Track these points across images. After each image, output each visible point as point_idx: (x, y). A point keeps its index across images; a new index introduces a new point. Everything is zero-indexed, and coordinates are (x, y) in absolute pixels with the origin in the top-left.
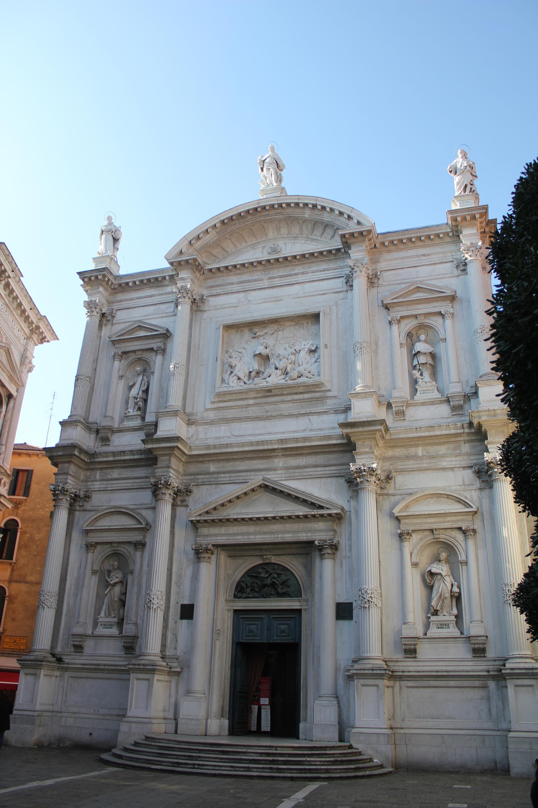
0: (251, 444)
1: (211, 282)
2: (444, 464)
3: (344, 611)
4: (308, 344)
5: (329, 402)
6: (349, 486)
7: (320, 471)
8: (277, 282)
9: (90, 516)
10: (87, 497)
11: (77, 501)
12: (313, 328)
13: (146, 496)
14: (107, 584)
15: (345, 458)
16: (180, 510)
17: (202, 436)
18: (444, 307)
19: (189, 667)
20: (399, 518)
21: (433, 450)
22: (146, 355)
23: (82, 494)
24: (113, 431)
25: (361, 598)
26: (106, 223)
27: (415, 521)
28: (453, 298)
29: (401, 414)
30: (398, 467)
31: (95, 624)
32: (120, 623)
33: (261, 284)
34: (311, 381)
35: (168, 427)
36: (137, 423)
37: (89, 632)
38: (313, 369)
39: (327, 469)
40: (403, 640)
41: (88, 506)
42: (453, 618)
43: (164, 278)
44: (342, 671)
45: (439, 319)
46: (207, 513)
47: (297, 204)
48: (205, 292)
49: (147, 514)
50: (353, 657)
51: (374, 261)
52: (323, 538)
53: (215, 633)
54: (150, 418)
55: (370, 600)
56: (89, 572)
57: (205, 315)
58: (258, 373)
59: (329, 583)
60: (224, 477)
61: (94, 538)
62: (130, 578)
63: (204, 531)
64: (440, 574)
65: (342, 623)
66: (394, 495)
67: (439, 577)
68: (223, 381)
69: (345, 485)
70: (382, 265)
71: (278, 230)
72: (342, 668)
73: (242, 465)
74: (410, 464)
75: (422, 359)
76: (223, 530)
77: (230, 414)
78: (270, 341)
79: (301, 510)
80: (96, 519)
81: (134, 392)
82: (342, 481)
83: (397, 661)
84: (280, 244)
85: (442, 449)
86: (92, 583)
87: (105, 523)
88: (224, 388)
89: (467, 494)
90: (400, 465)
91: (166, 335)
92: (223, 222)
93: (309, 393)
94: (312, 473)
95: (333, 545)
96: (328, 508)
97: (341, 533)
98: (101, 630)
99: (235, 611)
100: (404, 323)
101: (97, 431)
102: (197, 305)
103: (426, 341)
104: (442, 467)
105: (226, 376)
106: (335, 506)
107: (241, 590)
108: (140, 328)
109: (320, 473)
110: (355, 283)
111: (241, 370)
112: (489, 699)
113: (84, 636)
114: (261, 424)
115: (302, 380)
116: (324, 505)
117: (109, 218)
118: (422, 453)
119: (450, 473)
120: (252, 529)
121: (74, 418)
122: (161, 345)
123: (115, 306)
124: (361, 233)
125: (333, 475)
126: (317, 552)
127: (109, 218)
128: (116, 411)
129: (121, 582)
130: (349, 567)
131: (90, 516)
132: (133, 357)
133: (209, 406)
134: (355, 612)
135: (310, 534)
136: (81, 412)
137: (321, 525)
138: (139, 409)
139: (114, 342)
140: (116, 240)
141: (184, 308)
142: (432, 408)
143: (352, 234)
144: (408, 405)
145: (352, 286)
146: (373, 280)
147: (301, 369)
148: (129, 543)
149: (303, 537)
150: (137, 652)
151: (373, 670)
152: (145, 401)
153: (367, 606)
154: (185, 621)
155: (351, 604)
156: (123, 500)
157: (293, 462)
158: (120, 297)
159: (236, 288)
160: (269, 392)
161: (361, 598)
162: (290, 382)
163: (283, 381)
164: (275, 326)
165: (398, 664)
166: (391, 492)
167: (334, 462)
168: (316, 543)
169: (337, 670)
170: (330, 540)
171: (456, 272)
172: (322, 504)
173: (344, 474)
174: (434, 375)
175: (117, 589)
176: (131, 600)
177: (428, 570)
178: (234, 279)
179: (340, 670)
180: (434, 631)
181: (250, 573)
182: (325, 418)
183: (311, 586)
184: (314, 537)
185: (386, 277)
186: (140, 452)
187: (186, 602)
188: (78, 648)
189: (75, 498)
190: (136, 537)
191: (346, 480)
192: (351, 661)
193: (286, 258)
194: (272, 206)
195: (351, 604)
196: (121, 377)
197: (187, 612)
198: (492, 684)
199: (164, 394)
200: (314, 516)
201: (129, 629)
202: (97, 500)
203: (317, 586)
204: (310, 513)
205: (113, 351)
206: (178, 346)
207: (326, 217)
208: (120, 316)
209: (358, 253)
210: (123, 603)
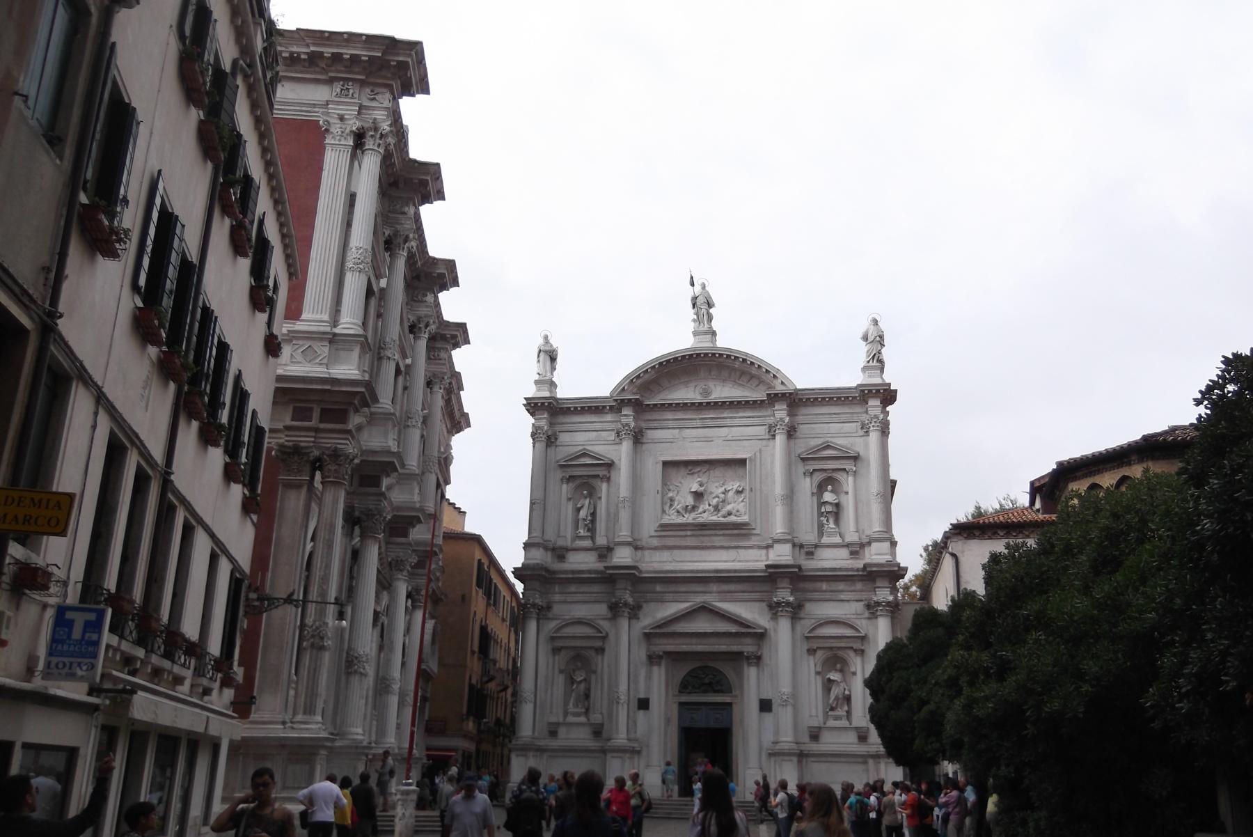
0: (692, 571)
1: (648, 416)
2: (842, 597)
3: (765, 706)
4: (735, 485)
5: (753, 538)
7: (746, 596)
8: (710, 423)
9: (553, 625)
10: (549, 608)
11: (543, 612)
12: (740, 471)
13: (602, 609)
14: (572, 681)
15: (766, 587)
16: (633, 621)
17: (647, 559)
18: (848, 465)
19: (648, 746)
21: (834, 586)
22: (592, 481)
23: (544, 605)
24: (568, 550)
26: (541, 341)
28: (856, 458)
29: (810, 554)
31: (566, 714)
32: (587, 712)
33: (694, 423)
34: (739, 520)
35: (623, 556)
36: (587, 543)
37: (561, 720)
38: (741, 507)
41: (550, 615)
43: (604, 407)
45: (845, 475)
46: (659, 627)
47: (729, 356)
48: (644, 425)
49: (605, 625)
51: (791, 414)
53: (668, 721)
54: (601, 540)
56: (557, 671)
57: (645, 447)
58: (694, 508)
59: (753, 685)
60: (669, 597)
61: (559, 644)
62: (593, 677)
63: (656, 641)
68: (664, 511)
69: (766, 609)
70: (800, 419)
71: (710, 371)
73: (683, 588)
74: (817, 595)
75: (829, 508)
76: (671, 641)
77: (671, 542)
78: (704, 479)
79: (733, 629)
80: (559, 629)
81: (583, 514)
84: (711, 384)
85: (841, 586)
86: (560, 680)
87: (570, 631)
88: (666, 520)
89: (858, 622)
90: (809, 595)
91: (610, 465)
92: (661, 364)
93: (737, 531)
98: (571, 719)
99: (681, 704)
100: (817, 474)
101: (553, 550)
102: (638, 438)
103: (832, 491)
105: (667, 508)
106: (761, 627)
107: (684, 687)
108: (584, 455)
110: (778, 438)
111: (678, 506)
112: (868, 771)
113: (558, 724)
114: (698, 552)
115: (732, 519)
117: (546, 337)
119: (846, 604)
120: (694, 641)
121: (537, 540)
122: (605, 473)
123: (558, 428)
124: (784, 394)
127: (546, 337)
128: (568, 531)
129: (585, 680)
131: (553, 625)
132: (578, 482)
133: (654, 534)
134: (774, 707)
136: (537, 534)
137: (748, 640)
138: (588, 530)
139: (562, 466)
140: (553, 359)
141: (626, 445)
142: (835, 551)
143: (776, 395)
144: (816, 546)
145: (774, 436)
146: (791, 433)
147: (729, 507)
148: (591, 648)
149: (735, 648)
150: (604, 735)
152: (593, 521)
154: (641, 712)
155: (770, 701)
156: (581, 611)
157: (725, 587)
158: (562, 419)
159: (671, 424)
160: (704, 527)
162: (722, 520)
163: (714, 518)
164: (707, 466)
167: (757, 589)
169: (761, 749)
171: (861, 433)
174: (837, 521)
175: (582, 686)
176: (596, 694)
178: (669, 415)
180: (831, 723)
181: (690, 673)
182: (751, 551)
183: (741, 686)
185: (803, 429)
186: (596, 572)
187: (642, 696)
188: (553, 734)
189: (541, 609)
190: (598, 644)
193: (716, 403)
194: (706, 354)
195: (770, 701)
196: (569, 499)
197: (644, 704)
198: (871, 761)
199: (613, 519)
201: (596, 718)
202: (557, 609)
205: (559, 474)
206: (623, 477)
207: (754, 371)
208: (564, 438)
209: (781, 412)
210: (587, 696)
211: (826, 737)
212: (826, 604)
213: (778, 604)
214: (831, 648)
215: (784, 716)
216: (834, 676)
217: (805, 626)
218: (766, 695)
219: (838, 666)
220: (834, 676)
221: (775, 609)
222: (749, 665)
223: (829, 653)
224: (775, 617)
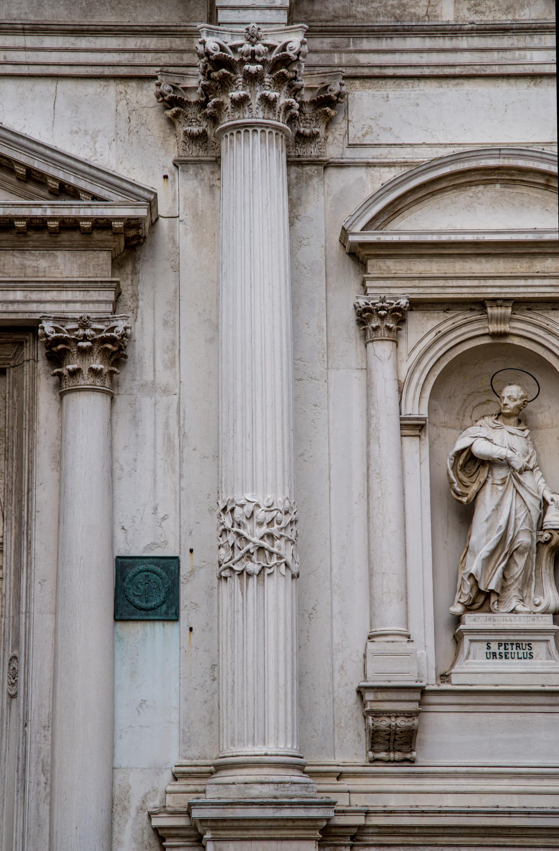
3: (145, 590)
6: (172, 122)
20: (363, 252)
25: (231, 538)
27: (421, 267)
30: (363, 59)
39: (83, 42)
40: (369, 696)
42: (547, 622)
44: (133, 812)
50: (174, 758)
52: (76, 310)
55: (266, 544)
64: (505, 463)
65: (136, 631)
66: (341, 166)
67: (500, 474)
69: (154, 118)
72: (135, 802)
82: (146, 95)
83: (340, 776)
90: (370, 54)
94: (21, 56)
95: (112, 340)
96: (95, 197)
97: (135, 296)
104: (529, 69)
109: (54, 57)
116: (82, 184)
118: (457, 10)
125: (107, 71)
126: (42, 365)
130: (167, 425)
134: (189, 592)
135: (19, 295)
137: (63, 264)
151: (279, 805)
153: (253, 567)
155: (170, 565)
161: (231, 538)
165: (346, 784)
166: (333, 151)
168: (48, 327)
169: (113, 807)
170: (100, 320)
172: (72, 180)
173: (152, 71)
177: (461, 444)
179: (125, 809)
180: (477, 668)
184: (34, 307)
191: (160, 95)
192: (168, 776)
195: (170, 565)
200: (37, 225)
203: (43, 496)
204: (24, 212)
211: (448, 738)
212: (451, 92)
213: (221, 68)
214: (479, 305)
215: (254, 626)
216: (491, 438)
217: (347, 197)
218: (140, 543)
219: (512, 393)
220: (491, 438)
221: (201, 110)
222: (63, 388)
223: (471, 330)
224: (203, 152)
